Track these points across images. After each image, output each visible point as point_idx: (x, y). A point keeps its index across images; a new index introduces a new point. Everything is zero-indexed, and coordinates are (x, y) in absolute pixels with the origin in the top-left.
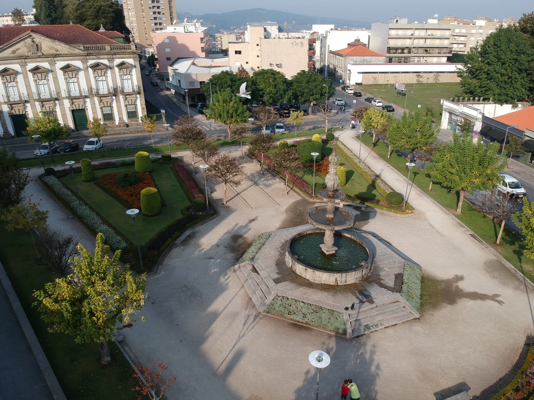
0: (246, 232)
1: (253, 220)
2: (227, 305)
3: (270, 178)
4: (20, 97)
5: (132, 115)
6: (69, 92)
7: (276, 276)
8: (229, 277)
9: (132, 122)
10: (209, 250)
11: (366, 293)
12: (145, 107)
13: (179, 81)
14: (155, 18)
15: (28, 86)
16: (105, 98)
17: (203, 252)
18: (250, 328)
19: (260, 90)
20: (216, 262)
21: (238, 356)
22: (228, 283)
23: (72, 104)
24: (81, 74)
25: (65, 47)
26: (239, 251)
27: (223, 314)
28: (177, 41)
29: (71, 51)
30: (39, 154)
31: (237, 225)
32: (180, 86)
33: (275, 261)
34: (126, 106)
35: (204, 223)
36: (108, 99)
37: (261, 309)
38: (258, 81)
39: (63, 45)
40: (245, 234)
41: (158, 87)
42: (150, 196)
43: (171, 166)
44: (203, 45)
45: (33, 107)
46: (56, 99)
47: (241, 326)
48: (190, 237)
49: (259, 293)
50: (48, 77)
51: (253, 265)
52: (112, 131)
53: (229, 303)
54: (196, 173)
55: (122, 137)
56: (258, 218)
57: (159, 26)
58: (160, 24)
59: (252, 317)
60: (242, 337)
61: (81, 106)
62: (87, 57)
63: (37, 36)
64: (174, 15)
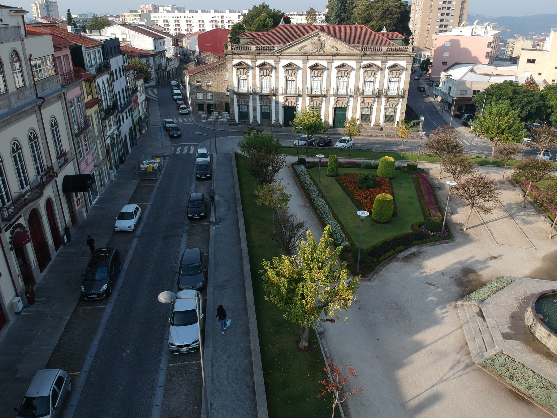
0: (482, 269)
1: (495, 258)
2: (437, 341)
3: (533, 213)
4: (295, 91)
5: (389, 118)
6: (337, 90)
7: (507, 330)
8: (447, 312)
9: (387, 126)
10: (432, 275)
12: (404, 111)
13: (450, 88)
14: (442, 20)
16: (368, 99)
17: (425, 275)
18: (456, 375)
19: (549, 108)
20: (436, 291)
22: (443, 318)
23: (337, 102)
24: (353, 74)
25: (345, 47)
26: (467, 287)
27: (429, 347)
28: (460, 45)
29: (349, 50)
30: (297, 144)
32: (449, 93)
33: (511, 313)
34: (386, 109)
35: (433, 245)
36: (370, 101)
37: (477, 360)
38: (549, 96)
39: (344, 45)
40: (479, 271)
41: (424, 93)
42: (384, 203)
43: (414, 176)
44: (489, 50)
45: (304, 101)
46: (324, 96)
47: (447, 369)
48: (414, 255)
49: (479, 341)
50: (323, 74)
51: (480, 307)
52: (365, 132)
53: (440, 339)
54: (440, 189)
55: (372, 140)
56: (502, 257)
57: (444, 27)
58: (446, 26)
59: (464, 364)
60: (445, 380)
61: (344, 104)
62: (363, 57)
63: (324, 35)
64: (464, 17)
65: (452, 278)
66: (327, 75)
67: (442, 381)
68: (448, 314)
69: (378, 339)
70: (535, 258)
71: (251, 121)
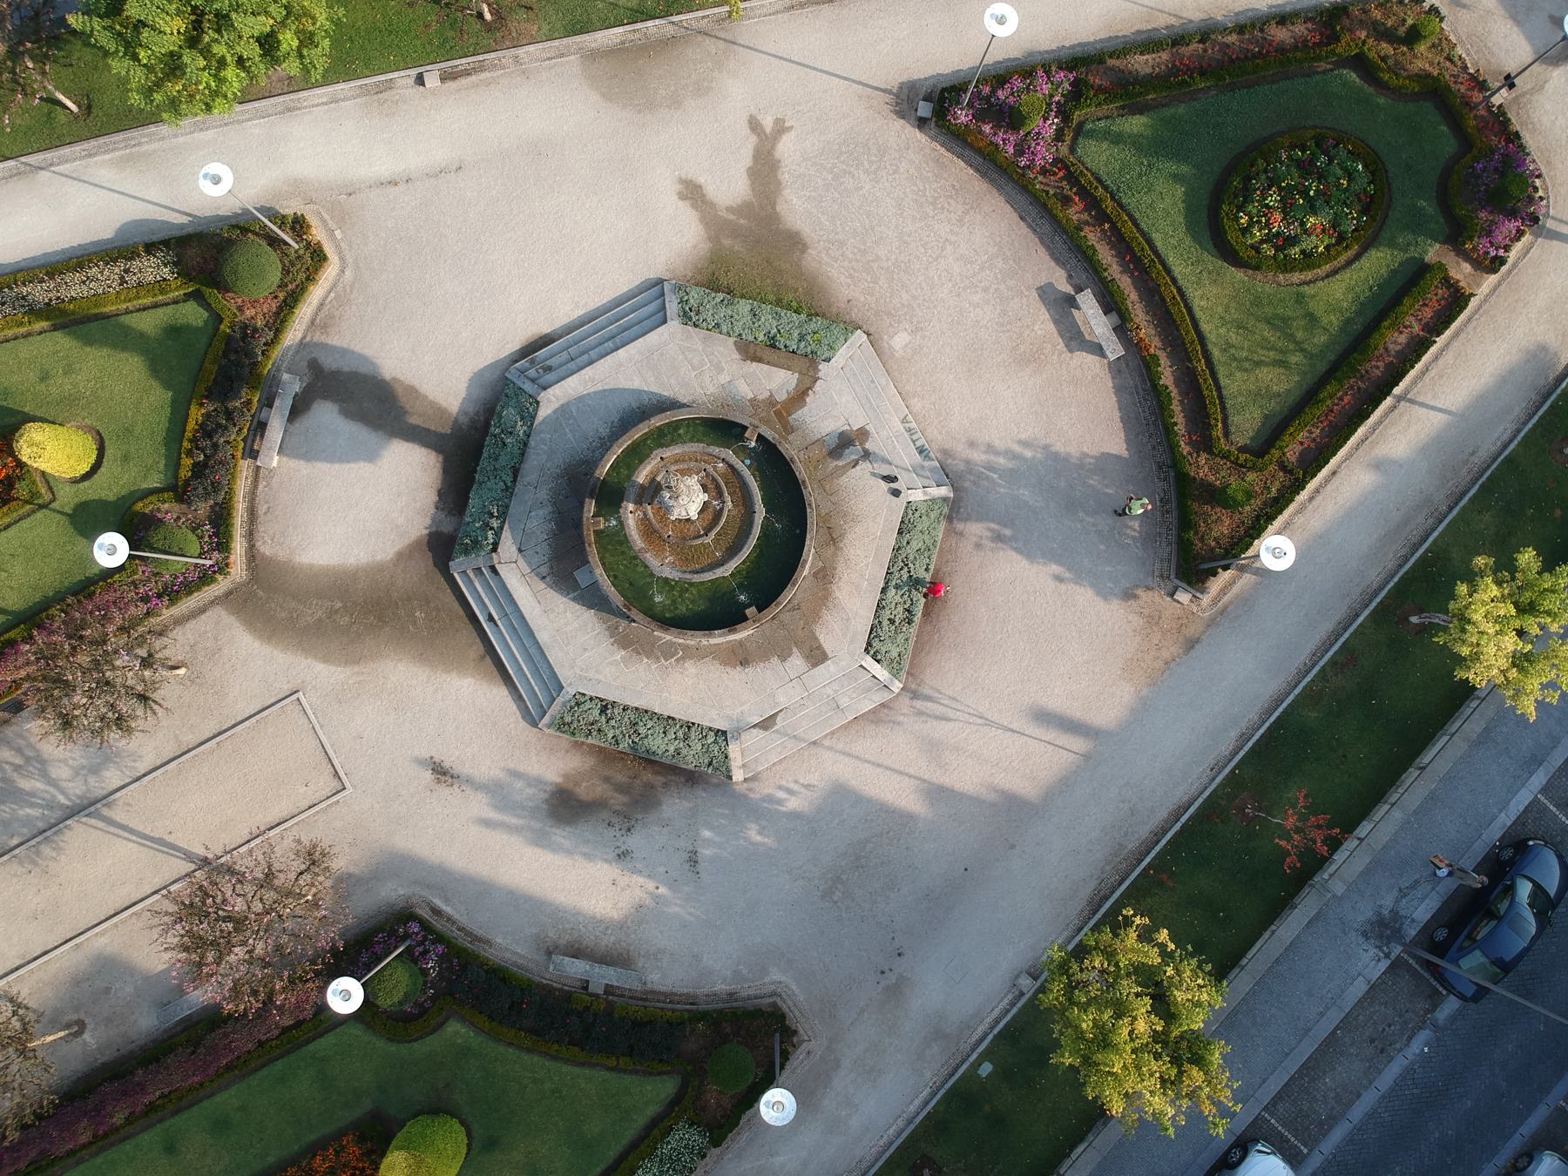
0: (538, 781)
7: (797, 662)
8: (780, 788)
11: (833, 442)
17: (663, 890)
20: (717, 839)
21: (1045, 717)
22: (807, 786)
31: (487, 823)
33: (728, 669)
35: (476, 939)
47: (950, 725)
48: (576, 952)
59: (919, 704)
65: (629, 830)
67: (987, 720)
68: (783, 783)
69: (966, 870)
70: (359, 682)
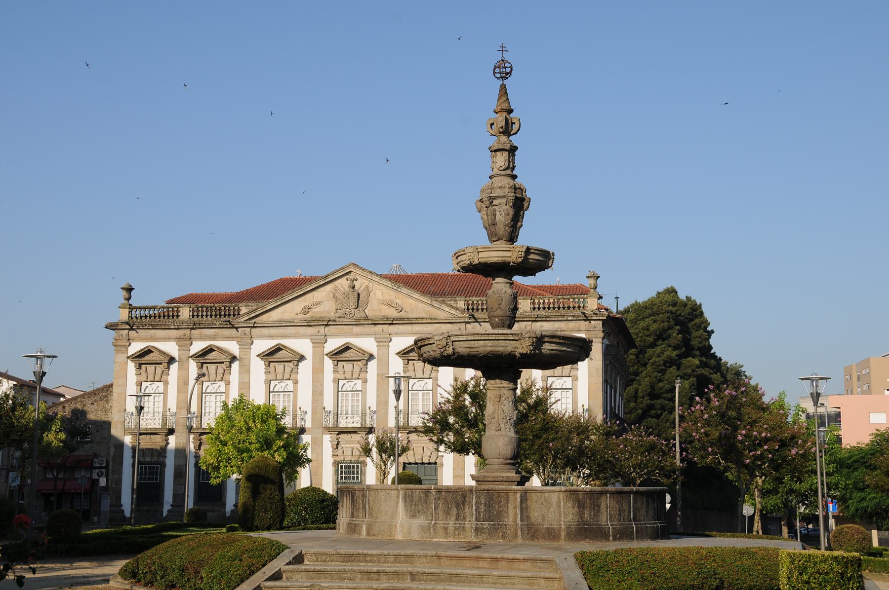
15: (317, 393)
66: (378, 376)
71: (167, 508)
